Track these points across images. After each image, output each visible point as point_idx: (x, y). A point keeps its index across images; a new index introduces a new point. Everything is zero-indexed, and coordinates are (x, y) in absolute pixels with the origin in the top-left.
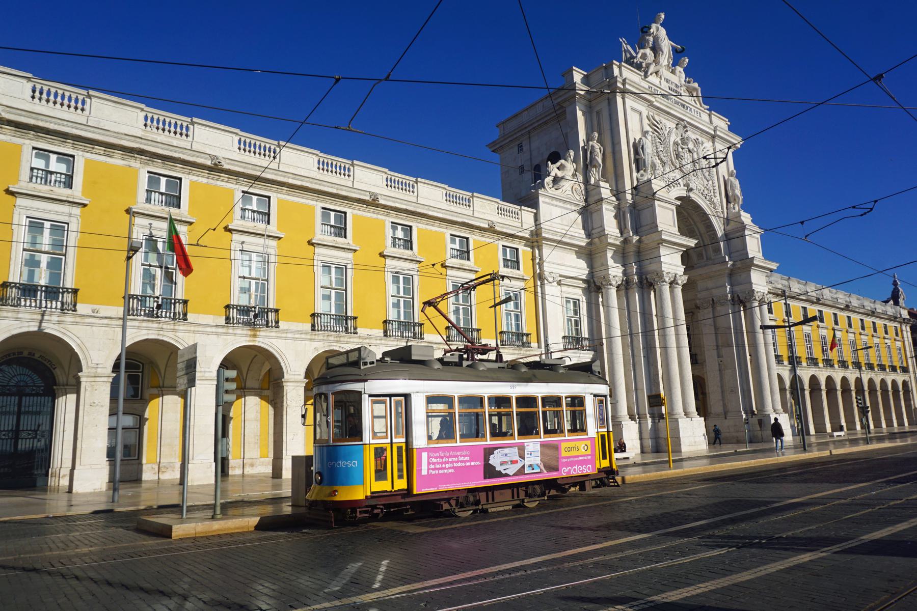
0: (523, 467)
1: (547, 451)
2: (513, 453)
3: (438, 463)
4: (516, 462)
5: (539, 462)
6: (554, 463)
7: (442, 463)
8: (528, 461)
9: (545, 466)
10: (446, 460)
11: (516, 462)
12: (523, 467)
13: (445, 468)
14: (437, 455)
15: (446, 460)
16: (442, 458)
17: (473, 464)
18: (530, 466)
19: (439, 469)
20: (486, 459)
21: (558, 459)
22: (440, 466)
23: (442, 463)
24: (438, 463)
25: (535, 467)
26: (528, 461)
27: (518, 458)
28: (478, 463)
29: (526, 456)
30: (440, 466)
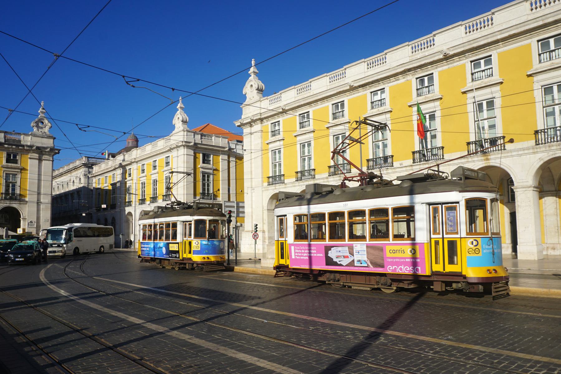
0: (353, 261)
1: (372, 251)
2: (345, 251)
3: (300, 253)
4: (347, 257)
5: (366, 259)
6: (379, 261)
7: (301, 253)
8: (356, 257)
9: (371, 263)
10: (303, 251)
11: (347, 257)
12: (353, 261)
13: (303, 256)
14: (299, 248)
15: (303, 251)
16: (301, 250)
17: (318, 255)
18: (359, 261)
19: (300, 256)
20: (326, 253)
21: (383, 258)
22: (300, 254)
23: (301, 253)
24: (300, 253)
25: (363, 262)
26: (356, 257)
27: (349, 255)
28: (321, 255)
29: (355, 254)
30: (300, 254)
